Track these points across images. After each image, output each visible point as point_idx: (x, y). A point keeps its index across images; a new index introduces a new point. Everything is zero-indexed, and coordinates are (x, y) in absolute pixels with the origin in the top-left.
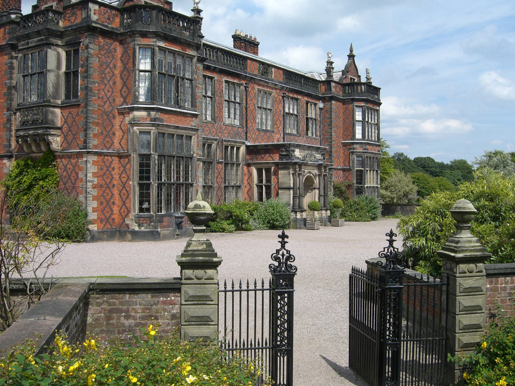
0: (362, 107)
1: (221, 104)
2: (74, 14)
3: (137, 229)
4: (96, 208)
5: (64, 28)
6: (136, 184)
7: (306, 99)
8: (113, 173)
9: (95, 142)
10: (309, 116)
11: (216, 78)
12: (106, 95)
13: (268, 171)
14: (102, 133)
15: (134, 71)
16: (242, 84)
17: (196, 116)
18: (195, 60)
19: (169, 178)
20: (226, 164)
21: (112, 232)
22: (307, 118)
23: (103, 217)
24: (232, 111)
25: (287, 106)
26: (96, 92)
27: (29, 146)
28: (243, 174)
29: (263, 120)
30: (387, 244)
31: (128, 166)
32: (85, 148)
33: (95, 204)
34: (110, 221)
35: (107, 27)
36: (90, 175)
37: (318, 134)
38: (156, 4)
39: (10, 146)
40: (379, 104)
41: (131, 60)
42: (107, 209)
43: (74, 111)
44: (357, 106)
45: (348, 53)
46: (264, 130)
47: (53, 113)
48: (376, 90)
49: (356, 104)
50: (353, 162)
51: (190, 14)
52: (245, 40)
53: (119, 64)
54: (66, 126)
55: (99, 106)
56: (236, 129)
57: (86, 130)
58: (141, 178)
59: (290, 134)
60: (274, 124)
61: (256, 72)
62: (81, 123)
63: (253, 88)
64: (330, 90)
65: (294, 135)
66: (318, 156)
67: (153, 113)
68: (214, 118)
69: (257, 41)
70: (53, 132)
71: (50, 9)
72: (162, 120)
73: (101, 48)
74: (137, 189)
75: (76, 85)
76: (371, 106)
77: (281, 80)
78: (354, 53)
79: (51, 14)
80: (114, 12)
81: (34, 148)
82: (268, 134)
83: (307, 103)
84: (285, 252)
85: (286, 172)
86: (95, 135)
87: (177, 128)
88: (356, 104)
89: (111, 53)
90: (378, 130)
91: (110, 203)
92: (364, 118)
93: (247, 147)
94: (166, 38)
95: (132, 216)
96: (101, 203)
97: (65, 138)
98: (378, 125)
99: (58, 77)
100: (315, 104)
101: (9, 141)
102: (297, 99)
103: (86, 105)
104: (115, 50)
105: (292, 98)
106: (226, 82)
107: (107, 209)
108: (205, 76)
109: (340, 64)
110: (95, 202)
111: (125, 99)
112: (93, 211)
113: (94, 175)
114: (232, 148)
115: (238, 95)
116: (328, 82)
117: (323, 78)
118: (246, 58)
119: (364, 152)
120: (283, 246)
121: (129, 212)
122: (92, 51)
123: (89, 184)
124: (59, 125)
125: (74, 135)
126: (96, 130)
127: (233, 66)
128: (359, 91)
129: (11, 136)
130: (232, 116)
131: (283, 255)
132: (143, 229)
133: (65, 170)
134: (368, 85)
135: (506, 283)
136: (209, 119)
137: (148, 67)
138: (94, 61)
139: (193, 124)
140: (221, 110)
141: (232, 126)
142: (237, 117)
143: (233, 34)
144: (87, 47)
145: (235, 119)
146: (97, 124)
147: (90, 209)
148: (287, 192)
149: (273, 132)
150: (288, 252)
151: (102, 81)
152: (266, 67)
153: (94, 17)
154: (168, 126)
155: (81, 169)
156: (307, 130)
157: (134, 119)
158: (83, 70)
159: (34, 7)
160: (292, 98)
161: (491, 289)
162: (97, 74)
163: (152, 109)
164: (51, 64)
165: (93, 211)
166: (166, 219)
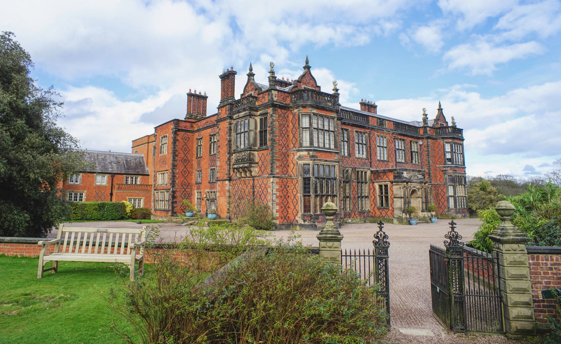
1: (354, 145)
3: (303, 223)
6: (302, 195)
7: (410, 139)
8: (288, 189)
9: (278, 171)
10: (413, 150)
11: (350, 130)
13: (386, 186)
14: (281, 165)
15: (299, 128)
18: (336, 119)
19: (322, 192)
20: (358, 183)
21: (288, 225)
22: (411, 152)
24: (361, 149)
25: (397, 144)
28: (370, 189)
29: (381, 154)
30: (450, 230)
31: (297, 185)
32: (272, 174)
34: (287, 218)
35: (283, 103)
36: (274, 190)
37: (420, 161)
38: (311, 88)
39: (230, 174)
40: (463, 140)
41: (297, 122)
42: (285, 211)
43: (265, 152)
44: (446, 142)
45: (438, 107)
46: (382, 161)
47: (253, 154)
48: (460, 131)
50: (446, 180)
51: (332, 92)
52: (368, 105)
53: (291, 125)
56: (363, 161)
58: (305, 192)
61: (375, 124)
62: (269, 158)
64: (427, 132)
65: (403, 163)
66: (420, 176)
67: (311, 153)
68: (349, 155)
69: (376, 104)
70: (253, 165)
71: (251, 96)
72: (317, 157)
74: (302, 198)
75: (266, 139)
76: (456, 141)
77: (392, 128)
78: (442, 107)
79: (251, 99)
80: (286, 94)
81: (243, 175)
82: (386, 163)
83: (411, 142)
84: (382, 233)
85: (398, 187)
86: (277, 167)
88: (445, 141)
89: (286, 118)
90: (463, 157)
91: (287, 207)
93: (372, 171)
94: (317, 108)
95: (300, 214)
96: (282, 207)
98: (463, 154)
99: (256, 134)
101: (229, 171)
102: (403, 140)
104: (288, 116)
107: (285, 211)
108: (342, 129)
109: (432, 116)
110: (278, 206)
114: (362, 172)
115: (364, 138)
116: (425, 128)
117: (422, 125)
118: (369, 116)
120: (381, 230)
121: (298, 212)
122: (274, 118)
124: (257, 161)
125: (265, 167)
127: (361, 121)
128: (447, 132)
129: (230, 168)
130: (361, 152)
131: (381, 235)
132: (306, 223)
133: (261, 188)
134: (454, 128)
135: (547, 260)
136: (346, 154)
138: (276, 123)
139: (336, 158)
140: (354, 149)
142: (365, 153)
144: (272, 116)
145: (363, 154)
146: (278, 160)
147: (274, 211)
148: (399, 200)
149: (388, 161)
150: (384, 233)
151: (281, 135)
152: (382, 121)
153: (275, 99)
155: (269, 187)
156: (412, 159)
157: (300, 157)
159: (242, 95)
160: (400, 139)
161: (534, 264)
163: (310, 150)
164: (252, 127)
166: (320, 217)
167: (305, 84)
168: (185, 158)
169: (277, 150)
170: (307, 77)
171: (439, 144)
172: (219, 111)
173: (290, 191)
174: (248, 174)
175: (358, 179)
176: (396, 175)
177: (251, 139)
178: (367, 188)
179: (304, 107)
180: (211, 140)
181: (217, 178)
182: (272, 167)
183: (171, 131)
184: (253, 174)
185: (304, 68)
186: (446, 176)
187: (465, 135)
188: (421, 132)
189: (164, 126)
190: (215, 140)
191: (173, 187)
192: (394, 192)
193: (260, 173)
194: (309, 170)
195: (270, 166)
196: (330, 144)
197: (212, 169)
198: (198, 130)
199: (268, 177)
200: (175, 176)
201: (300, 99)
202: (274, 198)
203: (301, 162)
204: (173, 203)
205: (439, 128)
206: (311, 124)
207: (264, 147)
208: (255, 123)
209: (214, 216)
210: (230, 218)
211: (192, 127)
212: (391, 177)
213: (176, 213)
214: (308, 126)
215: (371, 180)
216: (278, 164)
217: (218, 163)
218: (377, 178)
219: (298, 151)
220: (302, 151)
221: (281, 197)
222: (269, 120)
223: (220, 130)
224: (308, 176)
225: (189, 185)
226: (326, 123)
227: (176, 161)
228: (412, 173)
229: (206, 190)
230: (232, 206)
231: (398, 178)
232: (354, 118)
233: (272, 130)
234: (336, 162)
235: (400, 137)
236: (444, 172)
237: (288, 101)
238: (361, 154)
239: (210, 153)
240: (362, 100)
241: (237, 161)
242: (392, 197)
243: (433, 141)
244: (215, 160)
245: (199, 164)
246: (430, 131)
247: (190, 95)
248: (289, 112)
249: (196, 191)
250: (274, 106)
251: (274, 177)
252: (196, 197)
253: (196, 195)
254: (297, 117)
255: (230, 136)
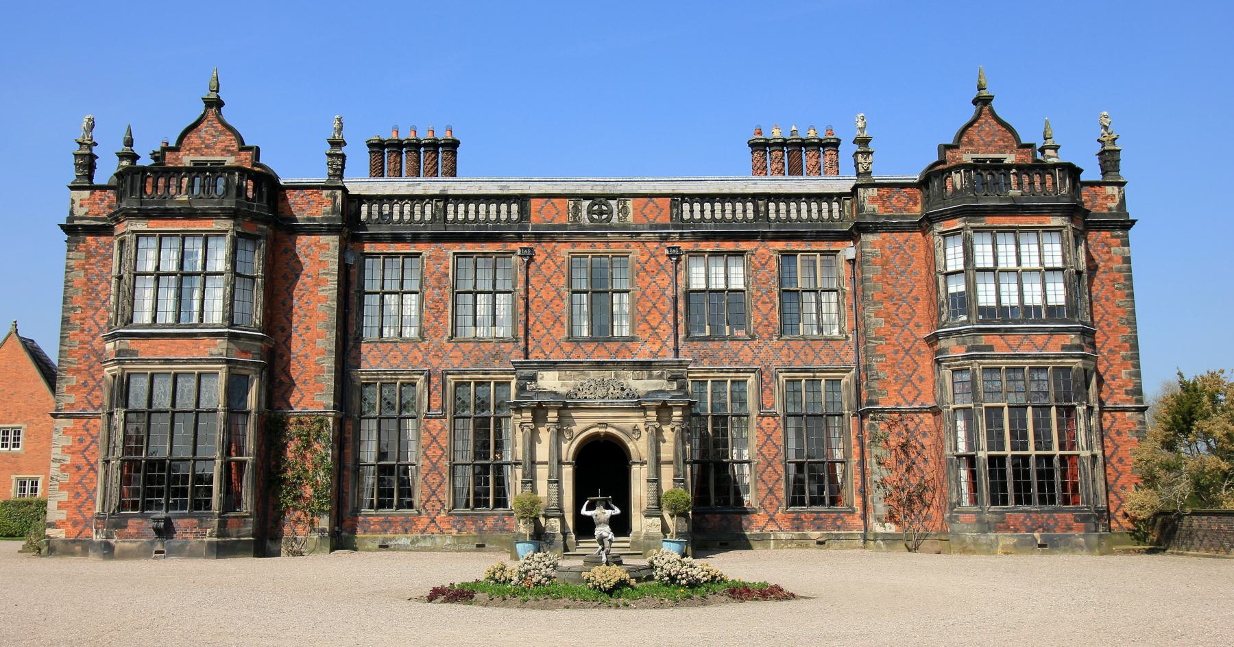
4: (65, 503)
7: (781, 245)
11: (426, 254)
12: (97, 324)
14: (85, 385)
16: (514, 253)
23: (80, 518)
26: (78, 322)
33: (64, 496)
49: (941, 229)
55: (81, 342)
72: (135, 353)
87: (168, 361)
88: (939, 228)
94: (145, 215)
112: (59, 508)
113: (65, 449)
119: (968, 358)
139: (215, 351)
146: (77, 371)
154: (146, 361)
162: (80, 294)
165: (59, 508)
221: (79, 468)
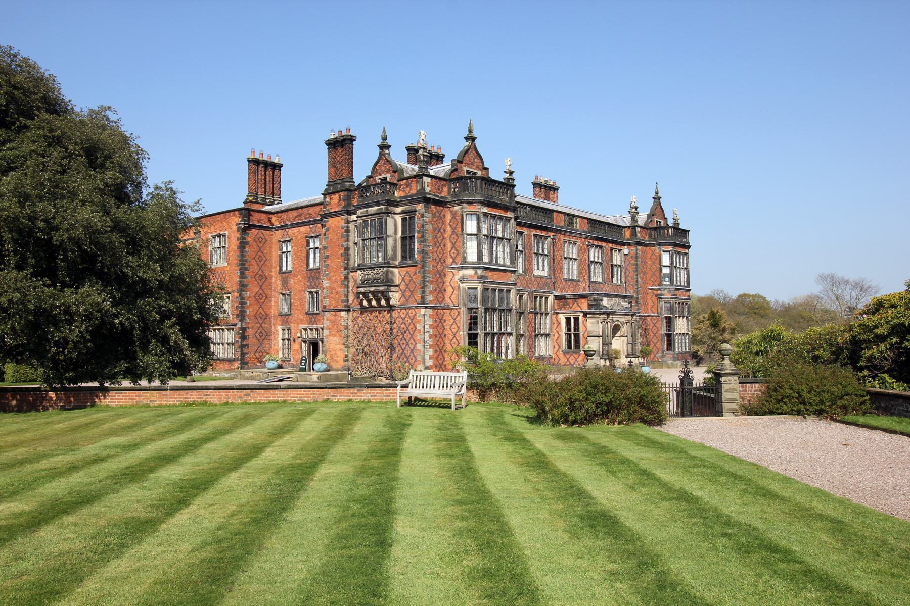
0: (669, 251)
2: (408, 186)
5: (400, 198)
6: (466, 334)
7: (610, 245)
10: (614, 262)
13: (577, 319)
15: (462, 235)
17: (514, 272)
19: (493, 328)
22: (612, 265)
25: (591, 253)
27: (369, 301)
28: (552, 323)
29: (571, 271)
31: (458, 318)
32: (423, 303)
36: (427, 327)
40: (688, 247)
41: (459, 225)
42: (441, 356)
43: (411, 270)
46: (570, 280)
47: (392, 272)
48: (685, 232)
50: (661, 309)
52: (545, 186)
54: (403, 283)
57: (423, 288)
58: (470, 329)
59: (595, 282)
60: (580, 273)
61: (562, 224)
62: (418, 280)
63: (560, 240)
64: (636, 235)
66: (626, 305)
67: (479, 272)
68: (525, 271)
69: (557, 185)
70: (392, 289)
73: (434, 215)
74: (467, 338)
75: (412, 250)
77: (586, 229)
80: (443, 182)
81: (374, 303)
82: (574, 283)
85: (594, 320)
86: (431, 292)
87: (499, 283)
88: (663, 248)
90: (688, 274)
92: (672, 263)
93: (555, 296)
96: (436, 351)
97: (403, 294)
100: (620, 251)
101: (347, 296)
102: (601, 247)
103: (423, 267)
105: (596, 246)
106: (535, 236)
111: (454, 259)
114: (541, 298)
115: (545, 246)
118: (553, 211)
122: (427, 219)
123: (427, 334)
124: (397, 283)
125: (412, 292)
126: (431, 287)
127: (542, 221)
128: (666, 235)
129: (348, 292)
133: (404, 322)
134: (676, 228)
137: (475, 231)
138: (429, 227)
141: (541, 277)
142: (546, 268)
143: (533, 180)
144: (423, 216)
146: (431, 282)
153: (428, 189)
154: (492, 283)
155: (419, 322)
156: (612, 276)
157: (463, 277)
158: (420, 235)
163: (479, 268)
164: (390, 230)
167: (468, 165)
168: (260, 273)
169: (429, 267)
170: (472, 154)
171: (653, 253)
172: (325, 198)
173: (448, 328)
174: (383, 302)
175: (535, 308)
176: (593, 302)
177: (390, 249)
178: (548, 321)
179: (470, 203)
180: (308, 245)
181: (325, 307)
182: (423, 292)
183: (235, 228)
184: (392, 302)
185: (467, 139)
186: (662, 303)
187: (692, 239)
188: (627, 234)
189: (219, 217)
190: (317, 245)
191: (241, 321)
192: (589, 329)
193: (403, 301)
194: (476, 297)
195: (419, 291)
196: (504, 259)
197: (311, 293)
198: (282, 228)
199: (417, 308)
200: (245, 303)
201: (464, 191)
202: (427, 338)
203: (464, 286)
204: (242, 347)
205: (655, 229)
206: (479, 229)
207: (409, 262)
208: (395, 224)
209: (324, 366)
210: (349, 369)
211: (270, 221)
212: (584, 305)
213: (247, 363)
214: (475, 232)
215: (555, 310)
216: (431, 287)
217: (326, 284)
218: (564, 306)
219: (461, 268)
220: (466, 268)
221: (436, 336)
222: (418, 221)
223: (328, 230)
224: (474, 305)
225: (266, 317)
226: (500, 227)
227: (246, 277)
228: (614, 300)
229: (301, 326)
230: (352, 350)
231: (595, 309)
232: (533, 214)
233: (423, 237)
234: (512, 285)
235: (596, 243)
236: (659, 297)
237: (445, 193)
238: (541, 270)
239: (308, 264)
240: (536, 178)
241: (365, 282)
242: (586, 335)
243: (644, 248)
244: (318, 278)
245: (285, 283)
246: (640, 232)
247: (255, 162)
248: (446, 209)
249: (279, 328)
250: (427, 201)
251: (426, 307)
252: (280, 336)
253: (279, 334)
254: (458, 218)
255: (348, 241)
